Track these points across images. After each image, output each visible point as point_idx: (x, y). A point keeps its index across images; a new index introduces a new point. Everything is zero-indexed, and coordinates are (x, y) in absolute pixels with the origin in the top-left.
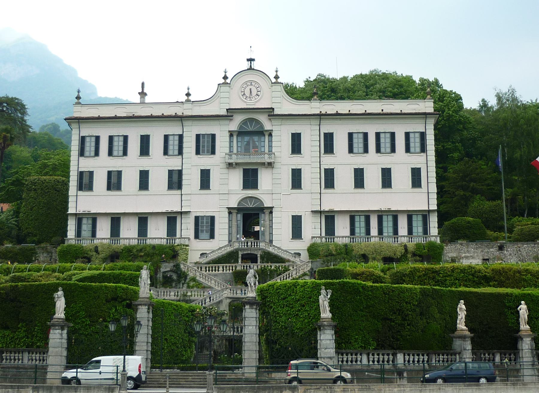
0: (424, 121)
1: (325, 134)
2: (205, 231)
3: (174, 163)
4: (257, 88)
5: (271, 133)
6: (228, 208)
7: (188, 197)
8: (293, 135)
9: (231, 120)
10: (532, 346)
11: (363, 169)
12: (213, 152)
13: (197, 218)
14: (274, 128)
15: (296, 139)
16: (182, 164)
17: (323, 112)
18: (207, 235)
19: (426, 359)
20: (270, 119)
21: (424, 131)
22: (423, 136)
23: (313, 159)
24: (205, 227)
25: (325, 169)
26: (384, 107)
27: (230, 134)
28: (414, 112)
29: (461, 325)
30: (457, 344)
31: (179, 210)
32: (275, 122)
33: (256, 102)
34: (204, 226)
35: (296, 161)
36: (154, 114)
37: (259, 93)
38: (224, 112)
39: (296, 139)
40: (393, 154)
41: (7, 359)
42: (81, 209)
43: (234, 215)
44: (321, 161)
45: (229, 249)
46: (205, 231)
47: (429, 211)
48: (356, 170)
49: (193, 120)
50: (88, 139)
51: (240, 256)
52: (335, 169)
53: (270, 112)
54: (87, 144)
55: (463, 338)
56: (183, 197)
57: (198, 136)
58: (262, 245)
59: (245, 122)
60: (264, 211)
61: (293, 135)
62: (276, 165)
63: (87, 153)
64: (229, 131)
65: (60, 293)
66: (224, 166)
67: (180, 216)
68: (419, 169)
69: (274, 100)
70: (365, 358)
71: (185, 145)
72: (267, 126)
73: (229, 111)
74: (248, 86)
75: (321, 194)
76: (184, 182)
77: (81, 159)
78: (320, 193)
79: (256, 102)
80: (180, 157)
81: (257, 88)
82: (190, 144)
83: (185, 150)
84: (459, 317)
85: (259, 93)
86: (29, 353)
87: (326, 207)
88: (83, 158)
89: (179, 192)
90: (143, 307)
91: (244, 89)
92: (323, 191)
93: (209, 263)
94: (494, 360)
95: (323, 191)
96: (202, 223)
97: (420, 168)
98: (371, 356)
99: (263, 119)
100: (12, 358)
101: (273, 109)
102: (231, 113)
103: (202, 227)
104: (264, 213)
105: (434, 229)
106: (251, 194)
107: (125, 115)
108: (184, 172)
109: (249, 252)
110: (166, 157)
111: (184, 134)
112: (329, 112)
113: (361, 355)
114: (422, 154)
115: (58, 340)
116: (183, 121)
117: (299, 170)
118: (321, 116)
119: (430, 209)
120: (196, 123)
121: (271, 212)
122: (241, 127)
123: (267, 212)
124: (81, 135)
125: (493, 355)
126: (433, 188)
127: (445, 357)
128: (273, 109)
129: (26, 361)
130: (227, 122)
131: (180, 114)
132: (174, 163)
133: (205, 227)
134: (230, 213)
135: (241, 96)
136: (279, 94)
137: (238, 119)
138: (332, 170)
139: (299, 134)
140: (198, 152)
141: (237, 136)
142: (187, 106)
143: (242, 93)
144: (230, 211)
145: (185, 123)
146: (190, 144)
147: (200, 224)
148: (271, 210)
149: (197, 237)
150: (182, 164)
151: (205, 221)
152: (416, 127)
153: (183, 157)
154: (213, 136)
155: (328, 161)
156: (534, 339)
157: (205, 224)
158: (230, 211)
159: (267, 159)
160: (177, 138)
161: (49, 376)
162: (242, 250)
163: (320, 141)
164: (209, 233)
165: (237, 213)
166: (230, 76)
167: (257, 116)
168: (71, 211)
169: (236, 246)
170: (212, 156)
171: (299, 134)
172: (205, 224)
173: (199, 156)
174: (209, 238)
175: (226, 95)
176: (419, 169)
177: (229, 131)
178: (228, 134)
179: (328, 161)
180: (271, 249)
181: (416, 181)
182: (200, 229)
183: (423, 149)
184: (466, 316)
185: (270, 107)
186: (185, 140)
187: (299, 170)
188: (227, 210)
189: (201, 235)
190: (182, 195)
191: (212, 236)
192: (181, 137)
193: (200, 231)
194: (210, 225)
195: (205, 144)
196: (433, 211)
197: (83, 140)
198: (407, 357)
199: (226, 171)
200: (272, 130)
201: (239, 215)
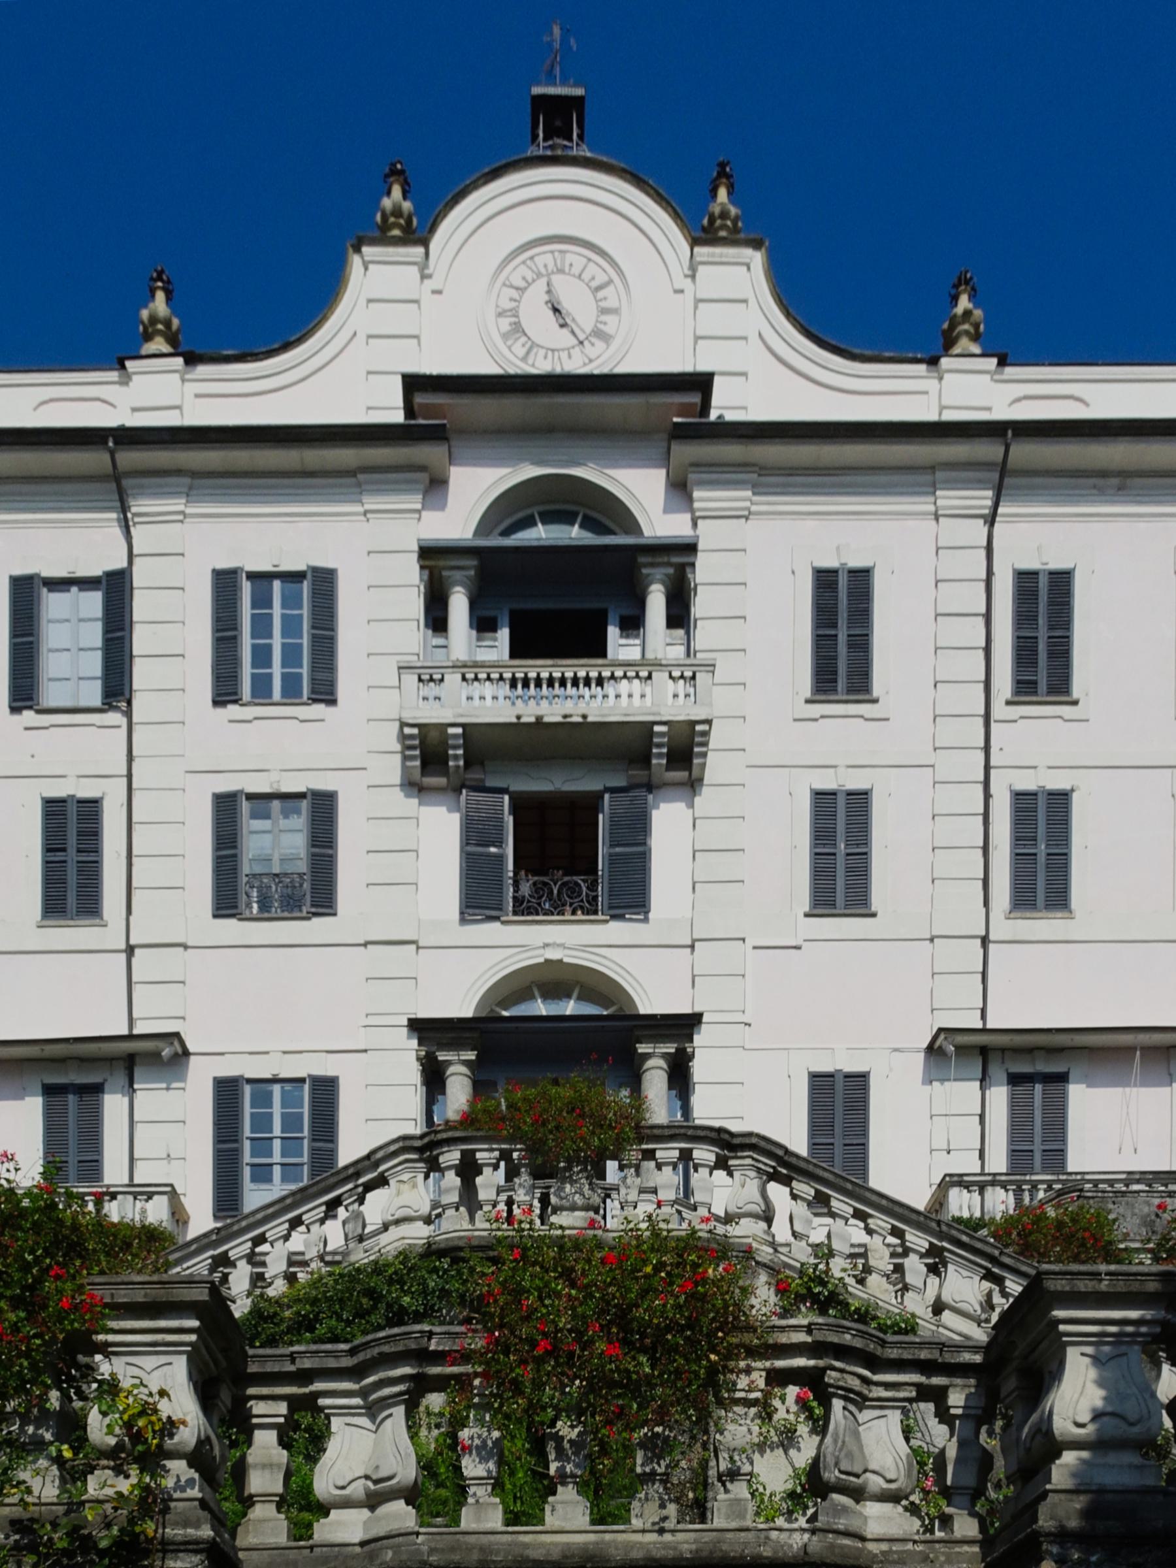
2: (277, 1170)
8: (825, 580)
23: (949, 732)
24: (277, 1144)
46: (277, 1170)
49: (195, 474)
52: (1075, 796)
56: (135, 961)
60: (642, 1048)
61: (825, 580)
67: (121, 1079)
75: (992, 947)
80: (115, 718)
83: (142, 674)
92: (1002, 927)
96: (262, 1122)
103: (262, 1145)
106: (563, 946)
111: (135, 569)
116: (126, 482)
117: (860, 801)
133: (277, 1144)
138: (1060, 801)
139: (861, 578)
147: (247, 1133)
151: (277, 1111)
153: (135, 719)
157: (277, 1130)
163: (988, 617)
170: (319, 709)
171: (861, 578)
172: (277, 1130)
182: (247, 1158)
186: (142, 606)
187: (860, 801)
190: (130, 950)
193: (247, 1171)
194: (306, 1133)
200: (690, 548)
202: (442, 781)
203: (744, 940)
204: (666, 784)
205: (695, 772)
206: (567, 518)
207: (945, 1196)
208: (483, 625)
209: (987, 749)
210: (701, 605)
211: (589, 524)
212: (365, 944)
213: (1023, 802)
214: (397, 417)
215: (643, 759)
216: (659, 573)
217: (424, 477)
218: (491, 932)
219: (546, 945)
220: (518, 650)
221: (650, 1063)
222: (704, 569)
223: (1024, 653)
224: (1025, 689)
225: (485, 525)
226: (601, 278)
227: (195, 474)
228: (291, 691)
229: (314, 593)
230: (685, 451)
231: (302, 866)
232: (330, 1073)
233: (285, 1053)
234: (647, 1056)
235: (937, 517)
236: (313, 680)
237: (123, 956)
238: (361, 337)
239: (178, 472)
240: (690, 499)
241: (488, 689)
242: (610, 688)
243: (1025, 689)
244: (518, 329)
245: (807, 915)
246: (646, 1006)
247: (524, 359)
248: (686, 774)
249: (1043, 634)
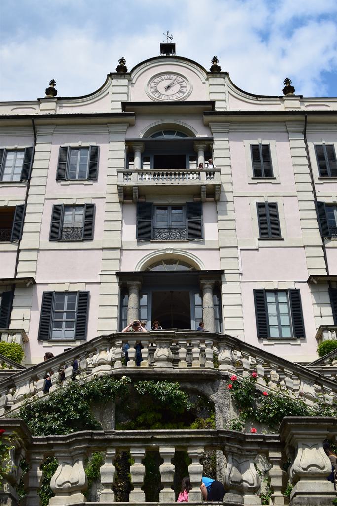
2: (64, 324)
4: (180, 82)
5: (209, 144)
6: (119, 274)
7: (33, 255)
13: (48, 296)
16: (27, 195)
24: (65, 315)
27: (127, 147)
35: (265, 191)
37: (184, 90)
44: (317, 191)
46: (64, 324)
49: (57, 124)
56: (20, 254)
59: (155, 131)
60: (202, 282)
71: (36, 164)
73: (127, 107)
74: (163, 80)
75: (326, 249)
76: (26, 228)
78: (323, 247)
81: (180, 82)
83: (34, 173)
85: (184, 90)
89: (14, 247)
91: (156, 84)
101: (212, 103)
108: (29, 209)
116: (36, 126)
117: (274, 206)
123: (208, 284)
133: (65, 315)
135: (151, 94)
142: (44, 106)
143: (153, 90)
144: (126, 280)
145: (41, 130)
150: (27, 195)
157: (65, 309)
158: (126, 280)
160: (21, 156)
164: (74, 329)
166: (129, 67)
167: (182, 121)
172: (65, 309)
173: (63, 183)
174: (73, 339)
186: (37, 156)
187: (274, 206)
190: (19, 251)
192: (29, 154)
202: (131, 201)
203: (237, 247)
204: (206, 201)
205: (217, 198)
206: (172, 133)
207: (322, 333)
208: (144, 159)
209: (314, 192)
210: (215, 154)
211: (179, 134)
212: (102, 249)
214: (120, 111)
215: (199, 195)
216: (201, 146)
217: (128, 124)
219: (167, 249)
220: (156, 166)
221: (206, 286)
225: (145, 135)
226: (181, 80)
227: (57, 124)
228: (82, 178)
229: (92, 152)
230: (207, 118)
231: (81, 225)
232: (87, 290)
233: (70, 283)
234: (204, 284)
235: (288, 133)
236: (89, 174)
237: (16, 253)
238: (110, 93)
239: (53, 124)
240: (210, 129)
241: (147, 177)
242: (187, 176)
244: (157, 91)
245: (258, 239)
246: (203, 268)
247: (158, 97)
248: (213, 199)
249: (327, 160)
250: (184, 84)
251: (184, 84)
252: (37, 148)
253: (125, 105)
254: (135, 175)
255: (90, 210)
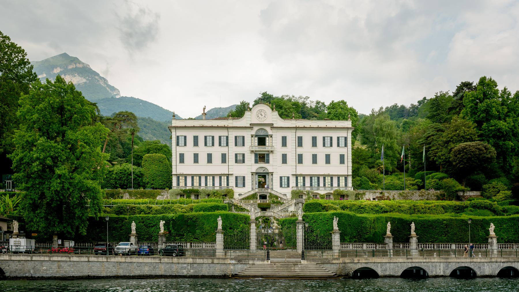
0: (346, 131)
1: (298, 137)
3: (224, 150)
7: (232, 167)
8: (283, 137)
9: (252, 129)
10: (416, 241)
11: (316, 155)
12: (244, 145)
13: (236, 177)
14: (273, 134)
15: (284, 139)
17: (298, 126)
18: (242, 185)
19: (374, 247)
20: (271, 129)
21: (346, 136)
22: (346, 139)
25: (298, 154)
26: (327, 124)
28: (342, 127)
29: (388, 233)
30: (387, 240)
31: (228, 173)
32: (274, 131)
33: (264, 120)
34: (240, 181)
35: (284, 150)
36: (214, 125)
38: (248, 125)
39: (284, 139)
40: (331, 147)
41: (194, 246)
42: (178, 172)
43: (254, 176)
45: (253, 192)
47: (348, 175)
48: (313, 155)
50: (180, 137)
51: (259, 195)
53: (271, 126)
54: (180, 140)
55: (388, 237)
57: (236, 137)
58: (269, 191)
61: (283, 137)
62: (274, 152)
63: (180, 145)
64: (251, 135)
65: (220, 218)
66: (249, 152)
68: (344, 155)
69: (273, 119)
70: (351, 245)
71: (229, 141)
72: (270, 132)
77: (177, 147)
79: (264, 120)
80: (227, 147)
82: (232, 141)
83: (229, 144)
84: (388, 229)
86: (205, 244)
87: (298, 173)
88: (178, 147)
90: (253, 224)
92: (297, 165)
93: (243, 199)
94: (400, 247)
95: (297, 165)
97: (344, 155)
98: (353, 245)
99: (268, 129)
100: (197, 246)
101: (273, 124)
102: (252, 126)
104: (269, 175)
105: (350, 184)
107: (199, 126)
109: (263, 194)
110: (220, 147)
112: (300, 126)
113: (349, 244)
114: (345, 148)
115: (221, 239)
118: (296, 128)
119: (349, 174)
120: (234, 130)
121: (272, 175)
122: (256, 132)
123: (270, 174)
124: (177, 135)
125: (400, 244)
126: (350, 164)
127: (382, 245)
128: (273, 124)
129: (204, 247)
130: (250, 130)
131: (226, 125)
132: (224, 150)
134: (252, 175)
136: (275, 117)
137: (256, 128)
138: (302, 155)
139: (286, 137)
140: (236, 145)
141: (255, 137)
145: (229, 130)
146: (232, 141)
148: (272, 174)
149: (237, 186)
152: (343, 134)
154: (243, 137)
155: (300, 150)
156: (418, 238)
159: (270, 149)
160: (225, 138)
161: (217, 254)
162: (259, 192)
165: (256, 175)
168: (174, 172)
169: (257, 190)
170: (243, 147)
171: (286, 137)
173: (236, 147)
175: (250, 117)
176: (344, 155)
177: (251, 135)
178: (251, 136)
179: (300, 150)
180: (273, 192)
181: (342, 161)
183: (346, 145)
184: (391, 229)
185: (271, 123)
186: (229, 139)
188: (251, 173)
189: (239, 185)
191: (244, 186)
192: (227, 137)
195: (240, 141)
196: (350, 175)
197: (178, 137)
198: (367, 246)
199: (250, 154)
201: (256, 176)
213: (298, 154)
218: (257, 164)
222: (273, 137)
223: (298, 143)
224: (299, 146)
243: (299, 146)
250: (265, 114)
251: (265, 114)
252: (229, 136)
253: (250, 124)
254: (254, 147)
255: (244, 155)
